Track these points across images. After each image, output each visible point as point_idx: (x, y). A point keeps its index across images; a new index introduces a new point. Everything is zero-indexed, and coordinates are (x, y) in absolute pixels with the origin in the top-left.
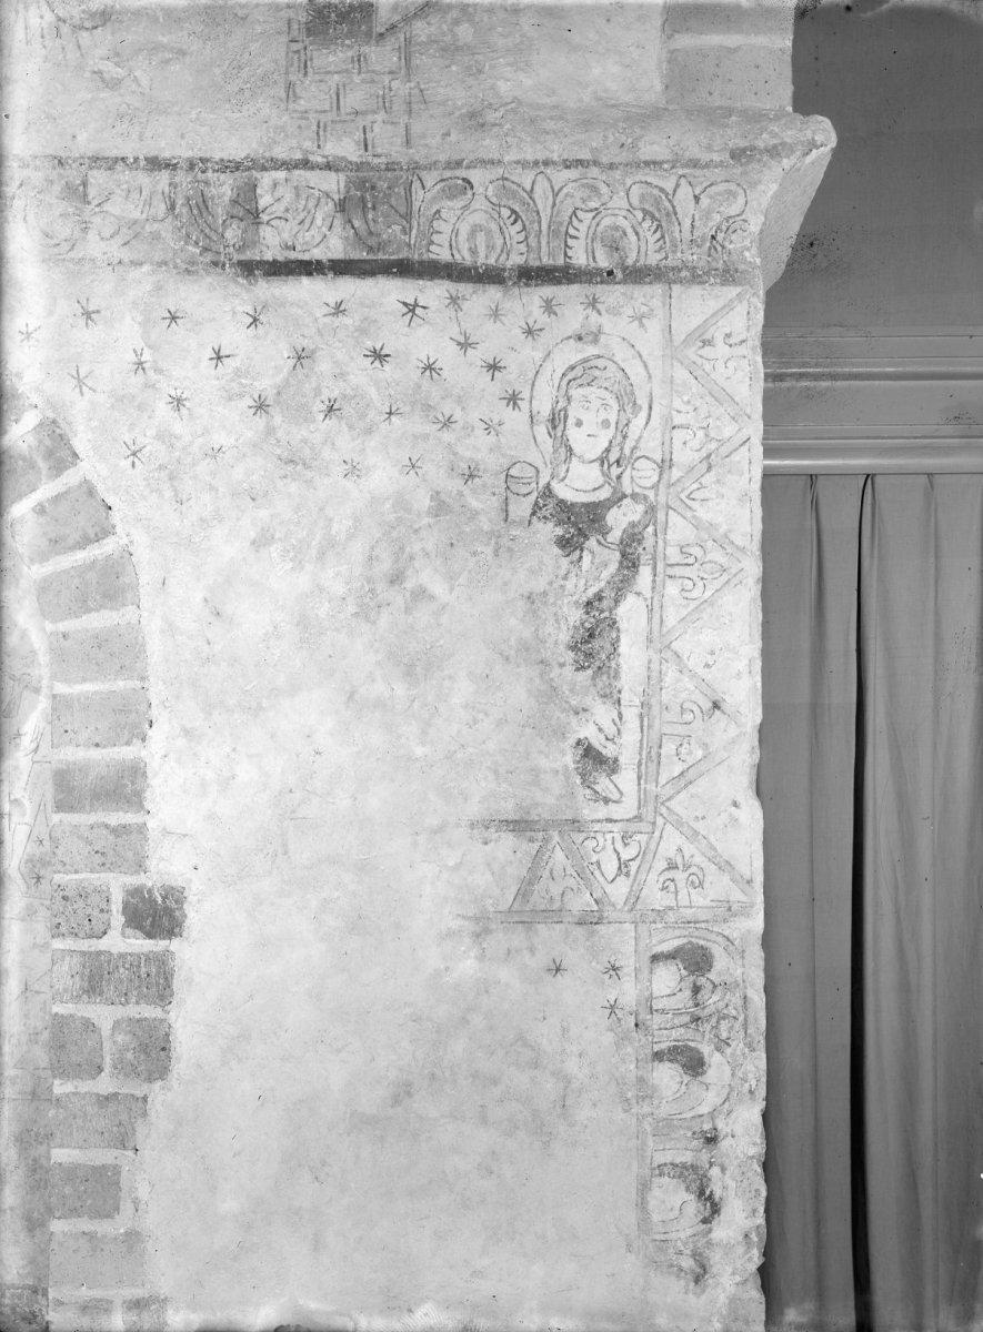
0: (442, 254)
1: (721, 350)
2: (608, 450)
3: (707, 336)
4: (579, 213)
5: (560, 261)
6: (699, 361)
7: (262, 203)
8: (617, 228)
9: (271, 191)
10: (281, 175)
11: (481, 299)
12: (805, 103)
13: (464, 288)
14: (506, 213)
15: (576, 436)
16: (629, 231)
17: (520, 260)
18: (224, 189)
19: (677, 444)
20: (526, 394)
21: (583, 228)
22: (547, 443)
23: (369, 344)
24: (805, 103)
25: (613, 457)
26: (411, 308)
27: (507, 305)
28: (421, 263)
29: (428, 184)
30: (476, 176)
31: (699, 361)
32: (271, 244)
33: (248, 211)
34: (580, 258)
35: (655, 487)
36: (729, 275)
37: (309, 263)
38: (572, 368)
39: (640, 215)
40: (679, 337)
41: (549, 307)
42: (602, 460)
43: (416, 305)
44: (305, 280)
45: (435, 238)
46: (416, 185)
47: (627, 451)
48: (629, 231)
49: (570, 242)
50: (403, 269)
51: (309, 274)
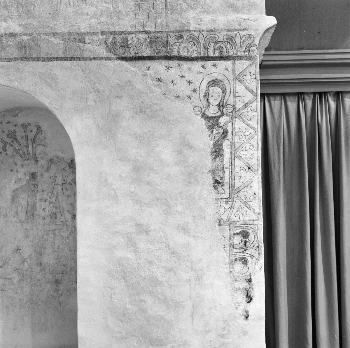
0: (175, 53)
1: (249, 77)
2: (220, 103)
3: (245, 73)
4: (211, 43)
5: (206, 55)
6: (243, 80)
7: (129, 43)
8: (221, 46)
9: (132, 40)
10: (133, 35)
11: (186, 65)
12: (268, 14)
13: (182, 63)
14: (192, 43)
15: (211, 100)
16: (224, 48)
17: (196, 55)
18: (119, 39)
19: (237, 101)
20: (198, 89)
21: (212, 47)
22: (204, 102)
23: (157, 77)
24: (268, 14)
25: (221, 104)
26: (168, 68)
27: (193, 67)
28: (170, 56)
29: (172, 37)
30: (183, 34)
31: (243, 80)
32: (131, 53)
33: (125, 45)
34: (211, 54)
35: (232, 112)
36: (249, 58)
37: (142, 57)
38: (210, 82)
39: (226, 43)
40: (237, 73)
41: (204, 67)
42: (218, 105)
43: (169, 67)
44: (140, 61)
45: (174, 50)
46: (169, 37)
47: (224, 103)
48: (224, 48)
49: (209, 50)
50: (167, 58)
51: (141, 60)
